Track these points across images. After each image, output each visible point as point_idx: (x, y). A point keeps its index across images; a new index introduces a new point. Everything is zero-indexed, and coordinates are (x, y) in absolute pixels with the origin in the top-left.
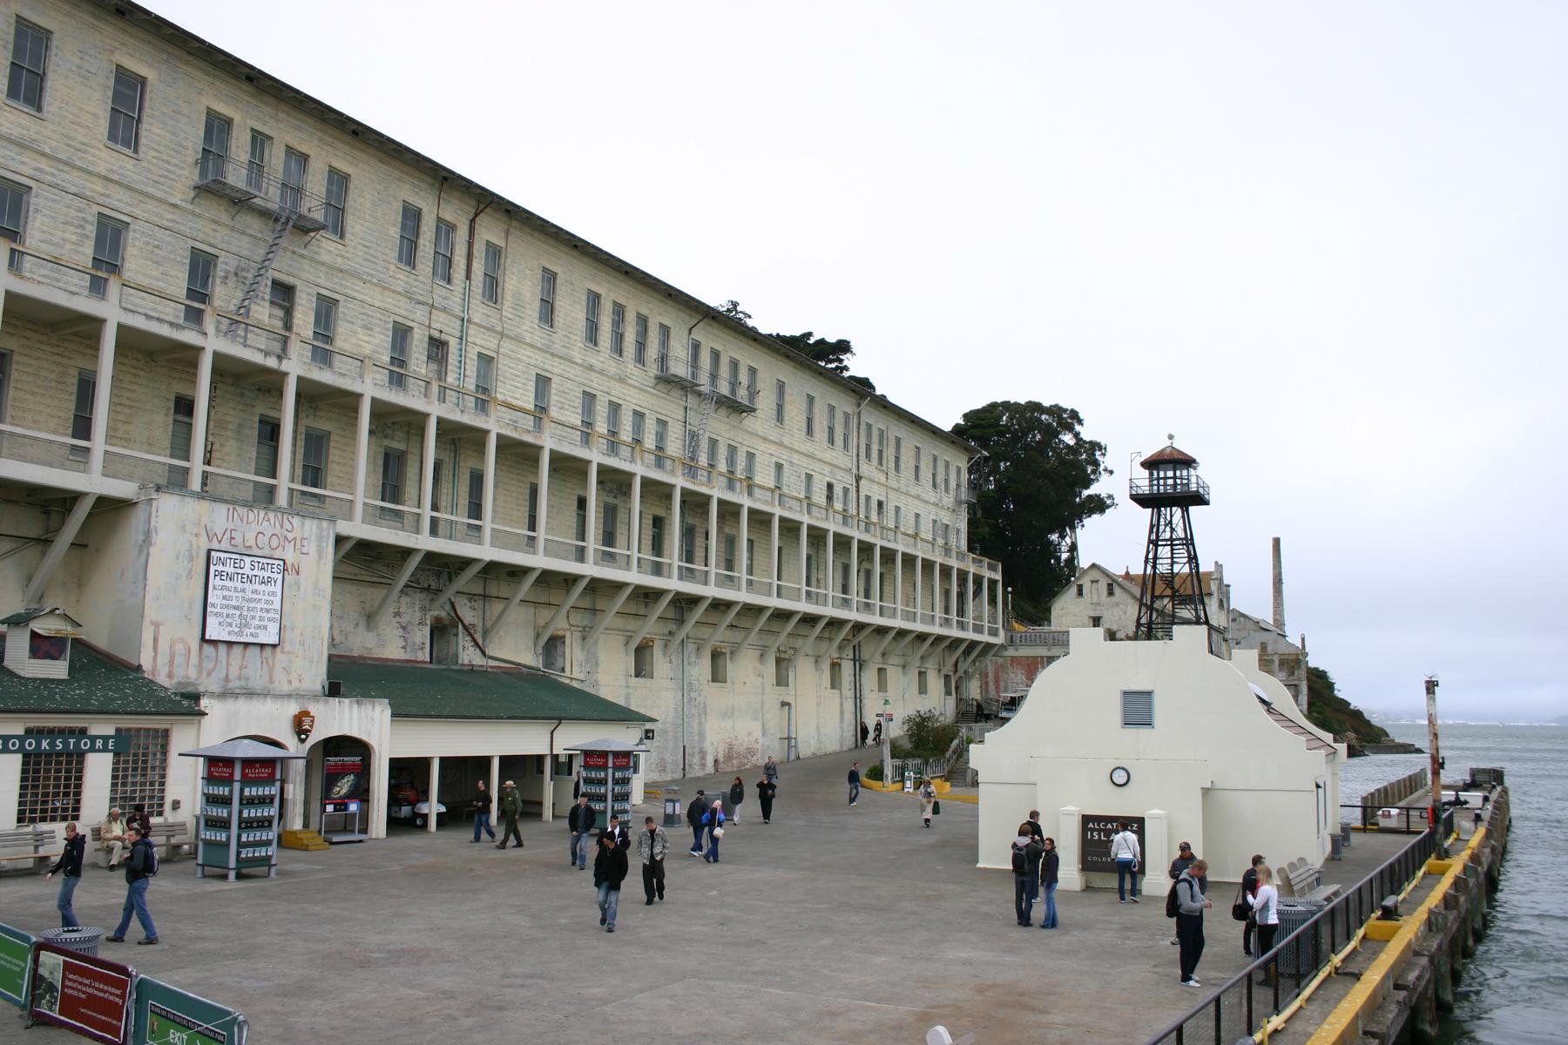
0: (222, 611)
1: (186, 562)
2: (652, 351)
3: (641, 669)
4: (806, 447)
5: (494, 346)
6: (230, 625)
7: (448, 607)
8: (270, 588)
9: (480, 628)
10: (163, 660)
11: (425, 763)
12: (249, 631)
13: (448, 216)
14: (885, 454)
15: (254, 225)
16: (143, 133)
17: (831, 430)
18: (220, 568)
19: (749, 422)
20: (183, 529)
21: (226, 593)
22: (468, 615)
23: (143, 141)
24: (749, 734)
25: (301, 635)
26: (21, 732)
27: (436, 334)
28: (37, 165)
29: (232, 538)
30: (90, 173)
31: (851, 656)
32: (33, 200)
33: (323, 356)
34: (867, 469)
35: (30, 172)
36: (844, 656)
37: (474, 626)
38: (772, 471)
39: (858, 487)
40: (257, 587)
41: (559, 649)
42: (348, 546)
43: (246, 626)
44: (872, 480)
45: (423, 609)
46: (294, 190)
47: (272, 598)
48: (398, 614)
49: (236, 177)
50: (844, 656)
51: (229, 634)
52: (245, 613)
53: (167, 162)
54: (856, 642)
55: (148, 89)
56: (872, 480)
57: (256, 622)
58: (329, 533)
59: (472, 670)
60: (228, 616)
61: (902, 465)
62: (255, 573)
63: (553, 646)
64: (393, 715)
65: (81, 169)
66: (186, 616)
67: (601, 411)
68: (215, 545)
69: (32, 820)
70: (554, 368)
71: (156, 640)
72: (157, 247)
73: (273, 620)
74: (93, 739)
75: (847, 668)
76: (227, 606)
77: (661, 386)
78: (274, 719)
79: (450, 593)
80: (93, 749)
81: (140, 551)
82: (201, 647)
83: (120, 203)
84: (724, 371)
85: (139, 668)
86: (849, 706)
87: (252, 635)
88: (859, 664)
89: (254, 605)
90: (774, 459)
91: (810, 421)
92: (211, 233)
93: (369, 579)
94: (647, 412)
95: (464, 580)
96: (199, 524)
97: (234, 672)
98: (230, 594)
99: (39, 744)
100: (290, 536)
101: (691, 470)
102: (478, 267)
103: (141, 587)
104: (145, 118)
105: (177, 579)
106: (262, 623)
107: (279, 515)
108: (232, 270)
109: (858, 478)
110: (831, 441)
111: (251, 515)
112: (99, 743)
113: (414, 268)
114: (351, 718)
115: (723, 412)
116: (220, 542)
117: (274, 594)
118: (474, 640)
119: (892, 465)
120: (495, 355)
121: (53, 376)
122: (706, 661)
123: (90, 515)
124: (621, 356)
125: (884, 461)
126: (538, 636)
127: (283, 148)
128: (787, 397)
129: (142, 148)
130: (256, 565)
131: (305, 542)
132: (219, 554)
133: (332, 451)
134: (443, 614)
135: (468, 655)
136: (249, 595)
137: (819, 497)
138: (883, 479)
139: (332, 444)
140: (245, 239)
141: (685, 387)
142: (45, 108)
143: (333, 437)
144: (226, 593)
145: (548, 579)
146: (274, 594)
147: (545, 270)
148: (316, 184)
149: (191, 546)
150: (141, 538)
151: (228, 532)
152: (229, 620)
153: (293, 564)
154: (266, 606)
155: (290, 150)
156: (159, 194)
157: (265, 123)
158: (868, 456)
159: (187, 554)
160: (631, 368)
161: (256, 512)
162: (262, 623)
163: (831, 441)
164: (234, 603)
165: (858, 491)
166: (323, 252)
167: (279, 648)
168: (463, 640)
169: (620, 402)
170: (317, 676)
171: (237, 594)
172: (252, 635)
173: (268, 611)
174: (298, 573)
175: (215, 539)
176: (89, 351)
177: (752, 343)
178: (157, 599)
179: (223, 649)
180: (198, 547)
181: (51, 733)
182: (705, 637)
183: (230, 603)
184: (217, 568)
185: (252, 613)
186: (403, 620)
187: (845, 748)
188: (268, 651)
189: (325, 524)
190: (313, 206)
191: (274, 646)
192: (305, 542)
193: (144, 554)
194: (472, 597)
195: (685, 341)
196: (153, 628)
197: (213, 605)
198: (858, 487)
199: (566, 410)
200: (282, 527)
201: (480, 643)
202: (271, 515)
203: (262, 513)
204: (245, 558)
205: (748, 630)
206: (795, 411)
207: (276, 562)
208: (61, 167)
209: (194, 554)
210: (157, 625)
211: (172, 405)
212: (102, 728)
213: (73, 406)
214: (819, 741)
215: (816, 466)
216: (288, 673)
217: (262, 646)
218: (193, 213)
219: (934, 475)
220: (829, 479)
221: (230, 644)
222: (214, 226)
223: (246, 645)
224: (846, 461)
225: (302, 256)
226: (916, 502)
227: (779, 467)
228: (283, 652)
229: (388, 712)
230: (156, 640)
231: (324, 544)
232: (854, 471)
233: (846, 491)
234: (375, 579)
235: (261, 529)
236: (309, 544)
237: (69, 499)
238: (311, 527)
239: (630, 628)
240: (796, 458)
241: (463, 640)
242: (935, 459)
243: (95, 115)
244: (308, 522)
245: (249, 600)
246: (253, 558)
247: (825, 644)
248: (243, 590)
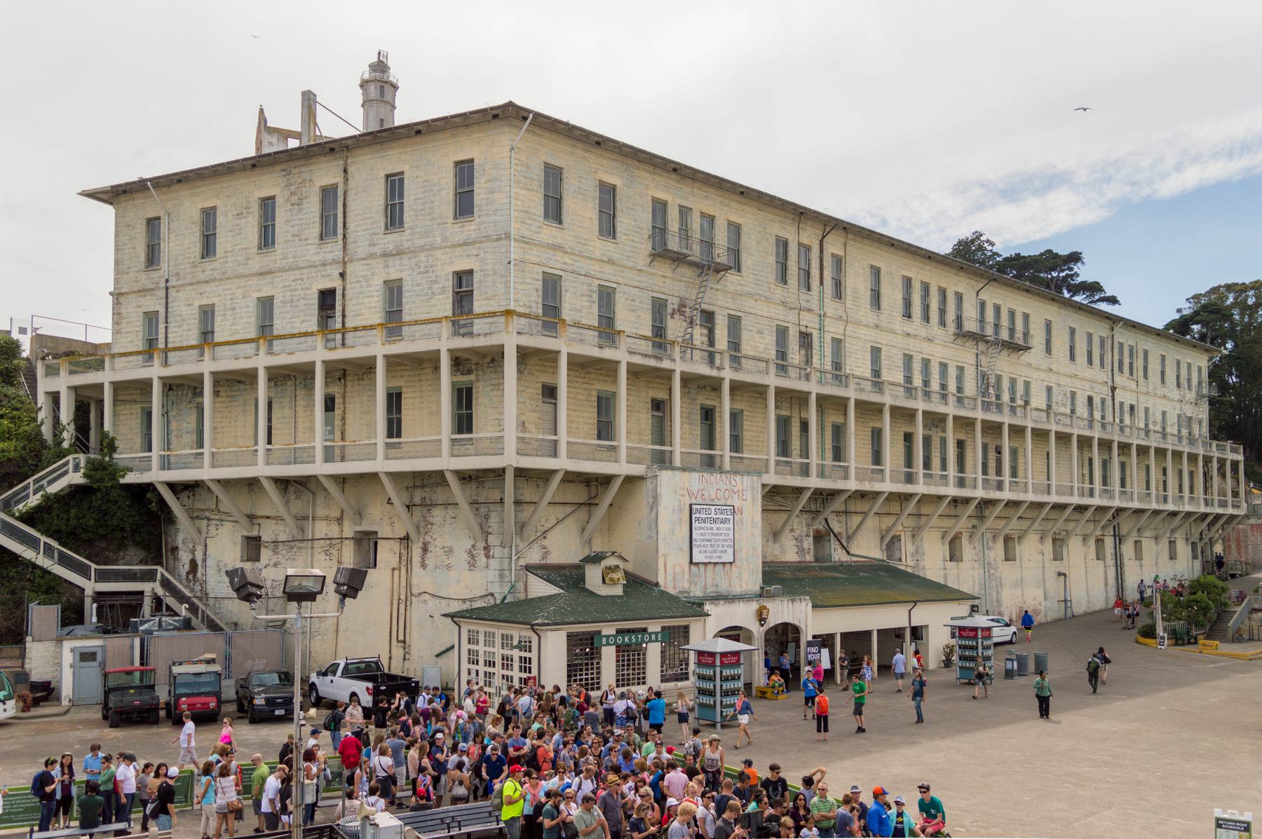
3: (954, 556)
4: (1071, 369)
5: (841, 331)
7: (823, 522)
8: (726, 526)
9: (844, 535)
10: (669, 578)
14: (1135, 366)
15: (685, 271)
16: (618, 225)
17: (1090, 353)
18: (698, 515)
19: (1026, 357)
20: (675, 493)
22: (836, 527)
23: (618, 229)
24: (1034, 599)
26: (614, 632)
27: (804, 329)
28: (563, 260)
30: (592, 259)
31: (1112, 533)
32: (563, 284)
33: (736, 360)
34: (1120, 380)
35: (559, 265)
36: (1106, 533)
37: (840, 533)
38: (1044, 393)
39: (1113, 396)
40: (719, 525)
41: (897, 545)
42: (767, 489)
44: (1124, 388)
45: (808, 525)
46: (708, 244)
48: (792, 530)
49: (674, 244)
50: (1106, 533)
53: (633, 241)
54: (1116, 523)
55: (618, 192)
56: (1124, 388)
59: (842, 567)
61: (1150, 372)
62: (718, 516)
63: (892, 544)
64: (814, 607)
65: (587, 258)
67: (917, 367)
68: (694, 501)
69: (623, 685)
70: (882, 339)
71: (665, 566)
72: (633, 300)
74: (650, 634)
75: (1109, 542)
77: (959, 341)
79: (827, 513)
80: (650, 641)
81: (652, 509)
83: (609, 275)
84: (1005, 321)
85: (657, 584)
86: (1112, 573)
88: (1119, 539)
90: (1046, 383)
91: (1072, 349)
92: (662, 284)
93: (772, 508)
94: (949, 362)
95: (838, 504)
97: (709, 582)
99: (624, 639)
100: (736, 489)
101: (986, 406)
102: (828, 274)
103: (654, 532)
104: (618, 213)
108: (676, 308)
109: (1113, 389)
110: (1090, 362)
112: (653, 637)
113: (786, 284)
115: (1005, 352)
118: (841, 544)
119: (1141, 373)
120: (842, 337)
121: (584, 397)
122: (1000, 545)
123: (620, 488)
124: (928, 322)
125: (1135, 371)
126: (882, 538)
127: (699, 214)
128: (1054, 332)
129: (618, 235)
133: (745, 423)
134: (821, 527)
135: (838, 555)
136: (715, 531)
137: (1082, 410)
138: (1133, 385)
139: (745, 418)
140: (682, 284)
141: (977, 337)
142: (564, 221)
143: (745, 413)
144: (702, 531)
145: (893, 497)
146: (728, 529)
147: (872, 267)
148: (721, 237)
150: (651, 501)
155: (703, 215)
156: (630, 265)
157: (686, 199)
158: (1121, 370)
163: (1090, 362)
164: (707, 537)
165: (1113, 400)
166: (729, 284)
168: (834, 544)
169: (930, 357)
176: (611, 379)
177: (1025, 294)
179: (702, 567)
181: (629, 631)
182: (999, 527)
186: (796, 534)
187: (1110, 606)
188: (728, 566)
189: (755, 478)
190: (721, 256)
191: (731, 563)
193: (655, 511)
194: (838, 513)
195: (974, 302)
198: (1113, 396)
199: (893, 373)
201: (845, 545)
202: (724, 476)
205: (1033, 520)
206: (1060, 342)
208: (577, 258)
211: (649, 406)
212: (654, 627)
213: (596, 415)
214: (1089, 602)
215: (1078, 384)
216: (741, 580)
218: (652, 274)
219: (1178, 377)
220: (1089, 393)
221: (706, 564)
222: (663, 280)
224: (1103, 376)
225: (717, 290)
226: (1163, 401)
227: (1049, 389)
229: (810, 605)
230: (665, 566)
232: (1110, 383)
233: (1103, 401)
234: (777, 508)
235: (718, 487)
237: (606, 480)
238: (747, 480)
239: (944, 525)
240: (1062, 380)
241: (834, 544)
242: (1178, 363)
243: (591, 218)
244: (745, 478)
247: (1091, 526)
248: (712, 529)
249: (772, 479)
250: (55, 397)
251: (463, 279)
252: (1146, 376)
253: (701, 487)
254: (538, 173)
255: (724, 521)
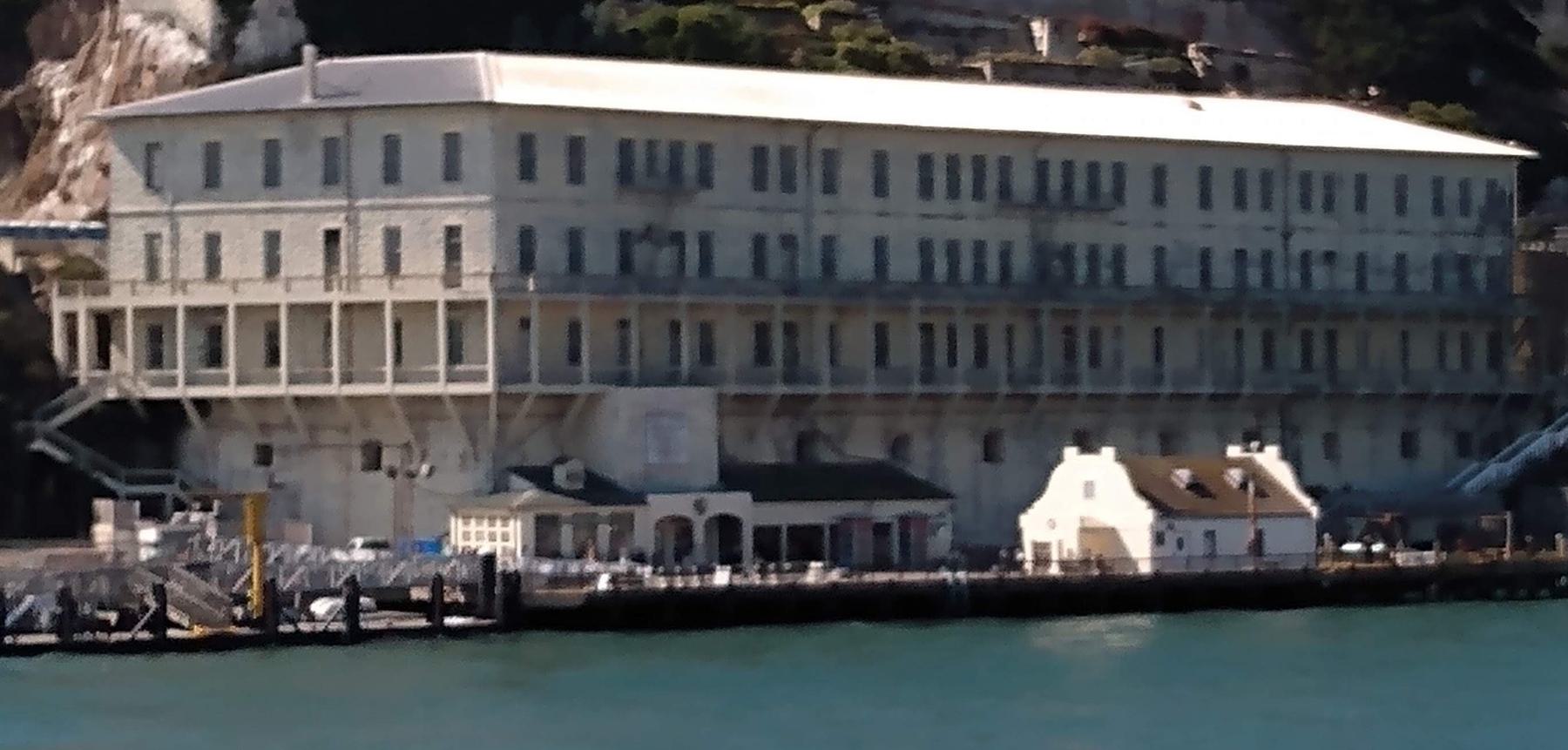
2: (991, 184)
3: (990, 452)
11: (777, 529)
13: (788, 142)
22: (825, 425)
63: (898, 445)
70: (888, 227)
78: (680, 505)
109: (1286, 236)
135: (827, 456)
160: (967, 204)
170: (713, 477)
198: (1286, 247)
249: (732, 389)
250: (71, 318)
251: (452, 232)
252: (1361, 205)
254: (514, 143)
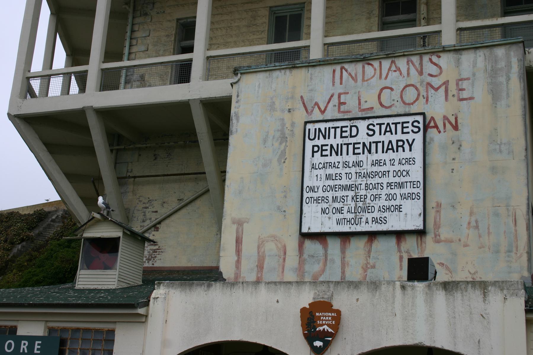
0: (326, 194)
1: (276, 144)
6: (340, 211)
12: (370, 216)
18: (321, 142)
20: (272, 107)
21: (330, 171)
25: (471, 214)
29: (341, 104)
40: (380, 156)
43: (366, 209)
47: (407, 167)
51: (338, 222)
52: (363, 192)
57: (383, 202)
58: (509, 65)
60: (335, 199)
62: (377, 137)
66: (279, 208)
68: (317, 115)
71: (239, 241)
73: (410, 196)
76: (333, 188)
82: (301, 246)
87: (375, 220)
89: (377, 180)
96: (292, 97)
98: (338, 171)
100: (436, 82)
105: (265, 166)
106: (393, 203)
107: (415, 59)
111: (369, 70)
114: (431, 315)
116: (323, 112)
117: (410, 161)
130: (377, 128)
131: (465, 85)
132: (318, 126)
146: (410, 161)
149: (283, 125)
151: (336, 97)
152: (337, 205)
153: (445, 118)
154: (397, 180)
159: (278, 134)
161: (376, 64)
162: (393, 203)
164: (345, 182)
167: (429, 239)
171: (348, 170)
172: (375, 220)
173: (401, 185)
174: (456, 128)
175: (316, 109)
178: (240, 192)
179: (334, 245)
180: (293, 124)
183: (338, 182)
184: (316, 142)
185: (375, 192)
191: (421, 233)
192: (465, 85)
196: (235, 227)
197: (312, 189)
200: (421, 73)
202: (402, 63)
203: (386, 64)
204: (356, 123)
207: (411, 119)
209: (287, 132)
210: (239, 223)
217: (400, 235)
223: (372, 235)
228: (438, 241)
230: (239, 241)
231: (502, 79)
235: (387, 83)
236: (473, 85)
245: (367, 175)
246: (371, 121)
248: (358, 164)
253: (339, 89)
255: (400, 145)
